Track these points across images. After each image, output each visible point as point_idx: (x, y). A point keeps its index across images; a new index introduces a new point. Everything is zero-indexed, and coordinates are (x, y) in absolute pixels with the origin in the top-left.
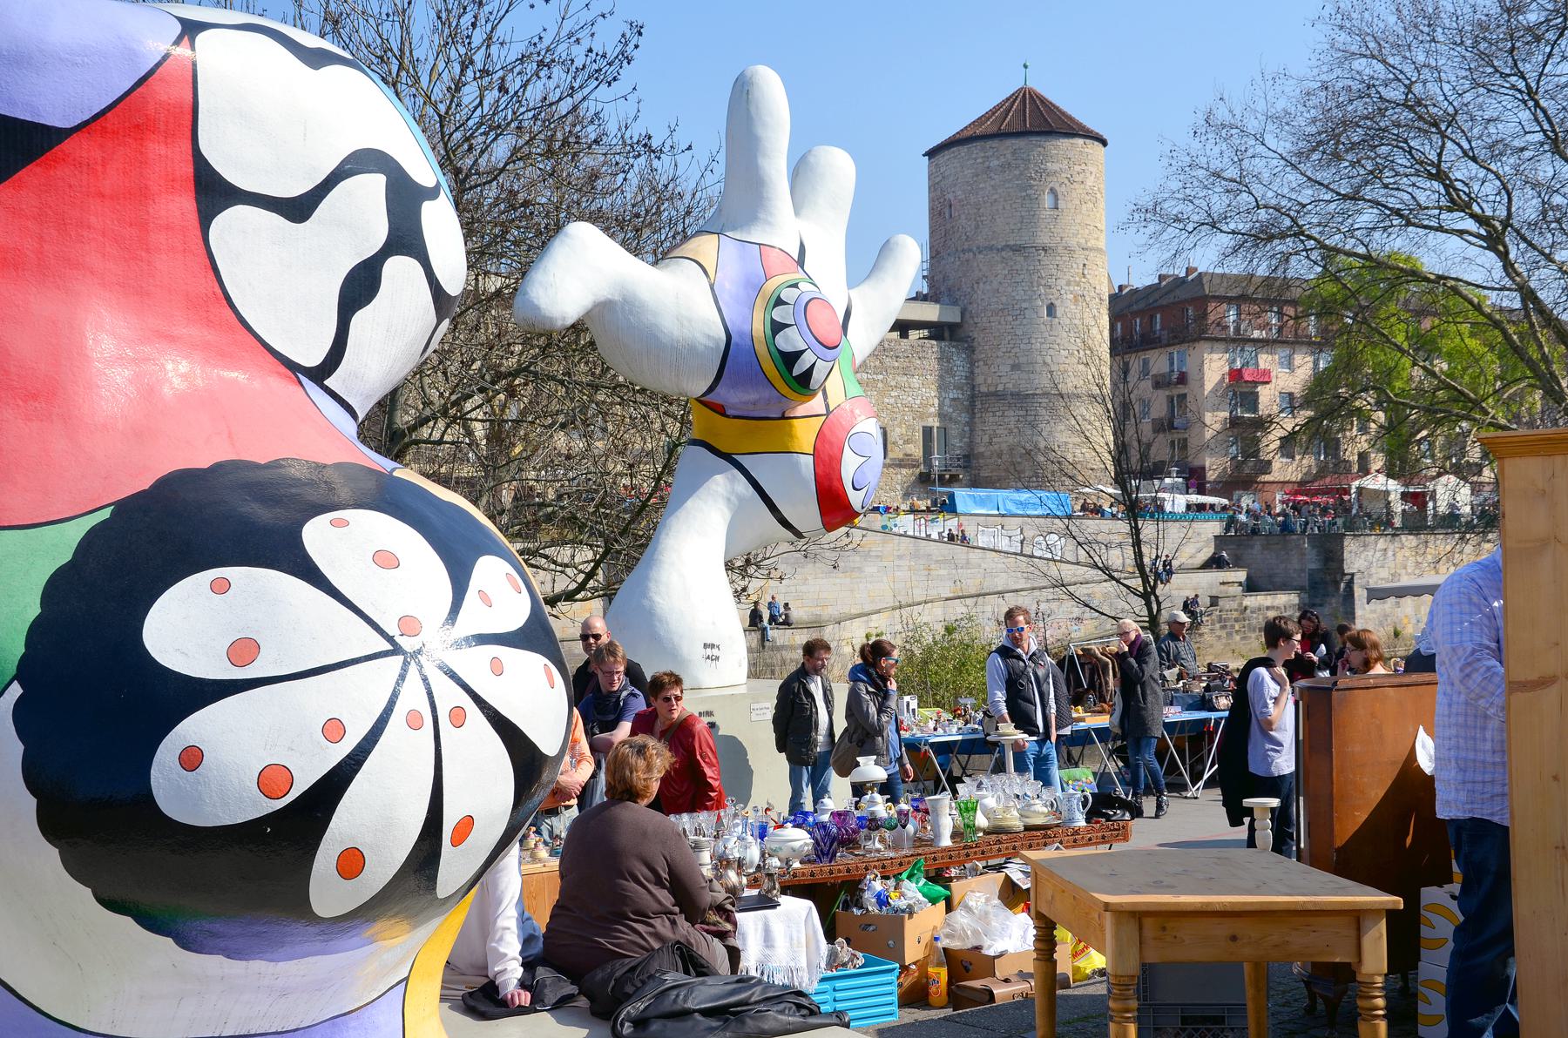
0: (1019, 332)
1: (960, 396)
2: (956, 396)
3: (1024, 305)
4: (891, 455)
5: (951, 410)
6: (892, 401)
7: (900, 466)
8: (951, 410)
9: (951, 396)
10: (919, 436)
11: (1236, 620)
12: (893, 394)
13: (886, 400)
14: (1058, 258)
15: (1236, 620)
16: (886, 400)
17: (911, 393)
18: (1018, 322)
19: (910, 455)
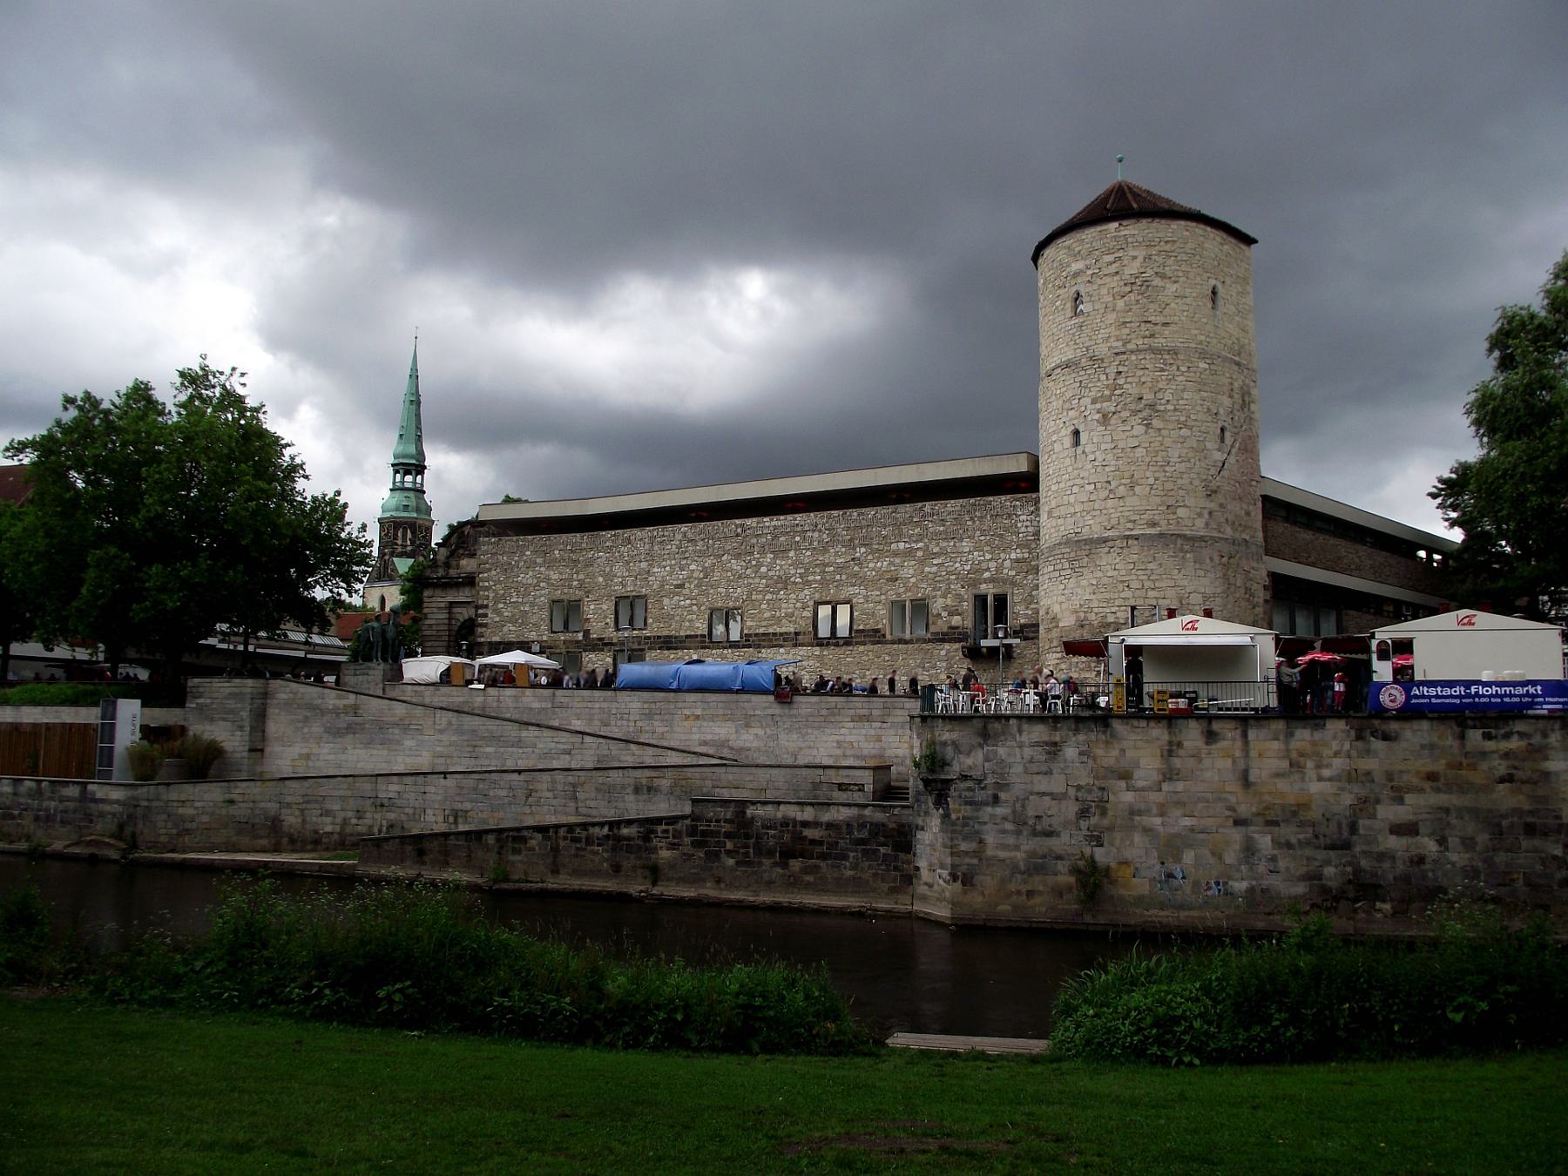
1: (1026, 555)
2: (1020, 556)
4: (932, 629)
5: (1014, 573)
6: (934, 569)
7: (943, 641)
9: (1013, 556)
10: (967, 606)
11: (728, 835)
12: (935, 562)
13: (927, 569)
14: (1082, 373)
15: (728, 835)
16: (927, 569)
17: (958, 559)
19: (957, 628)
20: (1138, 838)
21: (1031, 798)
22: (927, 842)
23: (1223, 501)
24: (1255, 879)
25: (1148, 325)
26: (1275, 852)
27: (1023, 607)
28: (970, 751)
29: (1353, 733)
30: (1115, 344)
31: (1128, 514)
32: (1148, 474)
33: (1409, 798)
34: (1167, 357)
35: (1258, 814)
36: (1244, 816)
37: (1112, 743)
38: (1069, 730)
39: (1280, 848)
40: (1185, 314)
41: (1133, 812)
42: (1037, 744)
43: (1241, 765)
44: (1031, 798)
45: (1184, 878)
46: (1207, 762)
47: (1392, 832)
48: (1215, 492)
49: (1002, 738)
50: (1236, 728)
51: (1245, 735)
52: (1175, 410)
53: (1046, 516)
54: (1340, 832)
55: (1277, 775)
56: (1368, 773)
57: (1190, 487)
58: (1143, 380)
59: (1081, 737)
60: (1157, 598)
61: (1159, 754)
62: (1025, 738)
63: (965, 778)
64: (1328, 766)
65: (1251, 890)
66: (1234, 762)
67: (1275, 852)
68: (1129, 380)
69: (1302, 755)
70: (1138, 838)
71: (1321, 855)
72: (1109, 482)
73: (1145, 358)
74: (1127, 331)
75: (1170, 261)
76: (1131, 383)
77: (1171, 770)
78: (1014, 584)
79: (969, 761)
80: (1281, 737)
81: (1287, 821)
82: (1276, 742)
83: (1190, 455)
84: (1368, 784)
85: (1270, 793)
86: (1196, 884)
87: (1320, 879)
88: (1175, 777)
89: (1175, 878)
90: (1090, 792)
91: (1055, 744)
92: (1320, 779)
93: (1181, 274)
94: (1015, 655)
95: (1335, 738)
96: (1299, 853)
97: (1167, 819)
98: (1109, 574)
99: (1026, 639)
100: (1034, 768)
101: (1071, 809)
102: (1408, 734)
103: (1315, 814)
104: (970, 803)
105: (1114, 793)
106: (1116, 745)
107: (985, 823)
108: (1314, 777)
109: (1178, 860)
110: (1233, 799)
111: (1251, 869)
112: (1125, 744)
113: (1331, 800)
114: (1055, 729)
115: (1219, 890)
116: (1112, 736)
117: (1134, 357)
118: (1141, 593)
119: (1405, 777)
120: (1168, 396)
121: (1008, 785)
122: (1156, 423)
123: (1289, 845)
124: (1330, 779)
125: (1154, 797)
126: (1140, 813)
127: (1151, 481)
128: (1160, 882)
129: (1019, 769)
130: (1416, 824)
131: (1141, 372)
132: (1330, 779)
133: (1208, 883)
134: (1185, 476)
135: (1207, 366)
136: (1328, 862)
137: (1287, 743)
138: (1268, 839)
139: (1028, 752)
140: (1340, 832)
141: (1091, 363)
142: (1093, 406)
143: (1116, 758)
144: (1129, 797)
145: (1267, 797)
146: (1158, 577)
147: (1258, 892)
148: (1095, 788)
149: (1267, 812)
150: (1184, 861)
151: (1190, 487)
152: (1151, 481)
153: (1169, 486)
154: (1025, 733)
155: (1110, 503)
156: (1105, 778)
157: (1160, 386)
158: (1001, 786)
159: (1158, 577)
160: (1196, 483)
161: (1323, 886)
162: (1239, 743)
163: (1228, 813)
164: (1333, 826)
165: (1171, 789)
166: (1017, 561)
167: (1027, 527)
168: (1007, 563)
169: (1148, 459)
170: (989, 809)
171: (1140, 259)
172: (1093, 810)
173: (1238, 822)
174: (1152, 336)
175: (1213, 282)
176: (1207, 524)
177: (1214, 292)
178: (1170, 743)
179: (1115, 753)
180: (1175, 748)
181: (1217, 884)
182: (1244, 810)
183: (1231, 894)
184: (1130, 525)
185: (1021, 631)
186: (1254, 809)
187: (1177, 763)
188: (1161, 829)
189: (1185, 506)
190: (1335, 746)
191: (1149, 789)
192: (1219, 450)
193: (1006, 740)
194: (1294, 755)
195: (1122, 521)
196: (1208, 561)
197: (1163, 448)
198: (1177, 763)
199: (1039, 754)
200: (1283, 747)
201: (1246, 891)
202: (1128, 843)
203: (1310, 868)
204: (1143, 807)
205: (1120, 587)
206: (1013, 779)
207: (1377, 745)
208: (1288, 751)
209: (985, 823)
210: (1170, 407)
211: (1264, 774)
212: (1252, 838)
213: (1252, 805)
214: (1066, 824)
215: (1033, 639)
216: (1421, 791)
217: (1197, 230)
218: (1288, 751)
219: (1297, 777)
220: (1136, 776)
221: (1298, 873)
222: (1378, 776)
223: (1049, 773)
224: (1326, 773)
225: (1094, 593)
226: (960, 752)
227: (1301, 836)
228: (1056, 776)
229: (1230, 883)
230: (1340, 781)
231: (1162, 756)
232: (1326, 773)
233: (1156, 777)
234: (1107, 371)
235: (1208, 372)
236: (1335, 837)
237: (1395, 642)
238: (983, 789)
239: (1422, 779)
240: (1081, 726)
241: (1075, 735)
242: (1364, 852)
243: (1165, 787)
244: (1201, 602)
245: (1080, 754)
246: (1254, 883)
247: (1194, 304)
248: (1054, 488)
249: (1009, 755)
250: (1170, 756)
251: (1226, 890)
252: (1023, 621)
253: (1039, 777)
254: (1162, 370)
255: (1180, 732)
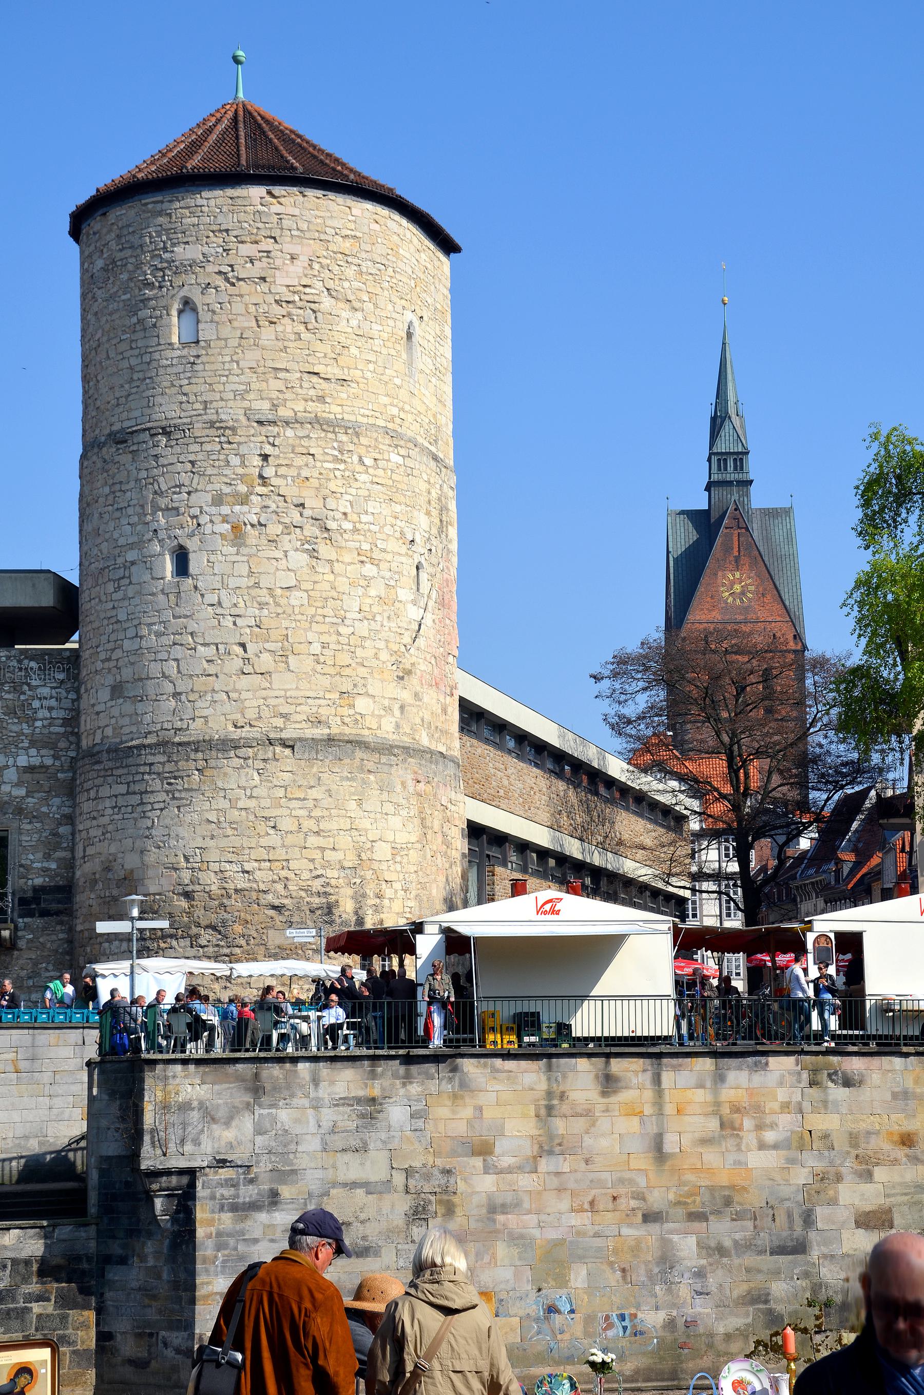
0: (122, 616)
1: (49, 761)
2: (36, 761)
3: (131, 556)
5: (22, 792)
8: (22, 792)
9: (22, 761)
14: (195, 448)
18: (120, 595)
20: (502, 1250)
21: (333, 1192)
22: (135, 1284)
23: (418, 688)
24: (674, 1305)
25: (315, 379)
26: (703, 1262)
27: (40, 855)
28: (231, 1118)
29: (805, 1075)
30: (257, 405)
31: (272, 702)
32: (311, 636)
33: (880, 1173)
34: (344, 438)
35: (678, 1203)
36: (656, 1207)
37: (462, 1097)
38: (395, 1076)
39: (710, 1256)
40: (371, 367)
41: (494, 1208)
42: (344, 1101)
43: (653, 1129)
44: (333, 1192)
45: (572, 1311)
46: (604, 1124)
47: (858, 1224)
48: (409, 672)
49: (285, 1093)
50: (644, 1071)
51: (657, 1080)
52: (356, 530)
53: (104, 695)
54: (791, 1228)
55: (705, 1141)
56: (826, 1136)
57: (374, 662)
58: (305, 473)
59: (415, 1089)
60: (323, 849)
61: (533, 1113)
62: (324, 1092)
63: (222, 1163)
64: (773, 1126)
65: (671, 1324)
66: (642, 1122)
67: (703, 1262)
68: (282, 471)
69: (736, 1109)
70: (502, 1250)
71: (768, 1262)
72: (243, 646)
73: (308, 436)
74: (280, 385)
75: (350, 272)
76: (285, 477)
77: (551, 1137)
78: (19, 811)
79: (229, 1135)
80: (708, 1084)
81: (717, 1213)
82: (700, 1092)
83: (375, 609)
84: (826, 1153)
85: (694, 1170)
86: (589, 1319)
87: (766, 1302)
88: (557, 1149)
89: (558, 1311)
90: (427, 1177)
91: (373, 1100)
92: (762, 1146)
93: (366, 298)
94: (22, 944)
95: (781, 1084)
96: (737, 1261)
97: (543, 1217)
98: (241, 804)
99: (44, 913)
100: (338, 1141)
101: (400, 1205)
102: (875, 1078)
103: (754, 1199)
104: (234, 1208)
105: (465, 1180)
106: (467, 1100)
107: (256, 1241)
108: (755, 1143)
109: (562, 1281)
110: (642, 1182)
111: (669, 1290)
112: (484, 1099)
113: (778, 1177)
114: (373, 1075)
115: (625, 1328)
116: (463, 1085)
117: (289, 433)
118: (298, 839)
119: (873, 1140)
120: (344, 506)
121: (294, 1172)
122: (325, 550)
123: (721, 1251)
124: (775, 1147)
125: (525, 1181)
126: (504, 1209)
127: (316, 648)
128: (537, 1320)
129: (312, 1144)
130: (890, 1211)
131: (300, 461)
132: (775, 1147)
133: (607, 1318)
134: (367, 643)
135: (400, 460)
136: (776, 1273)
137: (716, 1091)
138: (692, 1241)
139: (328, 1115)
140: (791, 1228)
141: (213, 432)
142: (214, 510)
143: (469, 1122)
144: (487, 1184)
145: (689, 1177)
146: (326, 813)
147: (680, 1322)
148: (436, 1172)
149: (689, 1201)
150: (572, 1284)
151: (374, 662)
152: (316, 648)
153: (344, 659)
154: (322, 1084)
155: (244, 682)
156: (454, 1154)
157: (332, 486)
158: (287, 1175)
159: (326, 813)
160: (384, 656)
161: (770, 1312)
162: (648, 1094)
163: (633, 1203)
164: (781, 1219)
165: (552, 1168)
166: (30, 769)
167: (50, 709)
168: (11, 775)
169: (312, 611)
170: (262, 1217)
171: (303, 261)
172: (432, 1208)
173: (649, 1217)
174: (321, 399)
175: (409, 316)
176: (398, 726)
177: (409, 335)
178: (549, 1094)
179: (468, 1112)
180: (555, 1102)
181: (622, 1317)
182: (657, 1199)
183: (641, 1333)
184: (279, 722)
185: (36, 899)
186: (671, 1196)
187: (559, 1125)
188: (536, 1233)
189: (367, 694)
190: (782, 1095)
191: (519, 1168)
192: (414, 602)
193: (292, 1096)
194: (726, 1110)
195: (266, 713)
196: (399, 788)
197: (335, 595)
198: (559, 1125)
199: (346, 1118)
200: (709, 1098)
201: (664, 1327)
202: (486, 1259)
203: (752, 1285)
204: (509, 1198)
205: (262, 827)
206: (302, 1162)
207: (837, 1093)
208: (717, 1104)
209: (256, 1241)
210: (347, 526)
211: (686, 1140)
212: (670, 1241)
213: (668, 1188)
214: (389, 1234)
215: (58, 913)
216: (895, 1162)
217: (390, 223)
218: (717, 1104)
219: (731, 1143)
220: (498, 1150)
221: (735, 1294)
222: (841, 1143)
223: (362, 1149)
224: (770, 1136)
225: (213, 837)
226: (214, 1120)
227: (737, 1236)
228: (372, 1153)
229: (640, 1315)
230: (789, 1148)
231: (537, 1116)
232: (770, 1136)
233: (529, 1149)
234: (243, 450)
235: (402, 469)
236: (785, 1234)
237: (839, 935)
238: (252, 1181)
239: (895, 1143)
240: (414, 1069)
241: (404, 1085)
242: (825, 1256)
243: (545, 1165)
244: (389, 857)
245: (412, 1116)
246: (674, 1313)
247: (384, 351)
248: (127, 644)
249: (297, 1121)
250: (549, 1115)
251: (634, 1326)
252: (38, 881)
253: (347, 1157)
254: (336, 460)
255: (564, 1077)
